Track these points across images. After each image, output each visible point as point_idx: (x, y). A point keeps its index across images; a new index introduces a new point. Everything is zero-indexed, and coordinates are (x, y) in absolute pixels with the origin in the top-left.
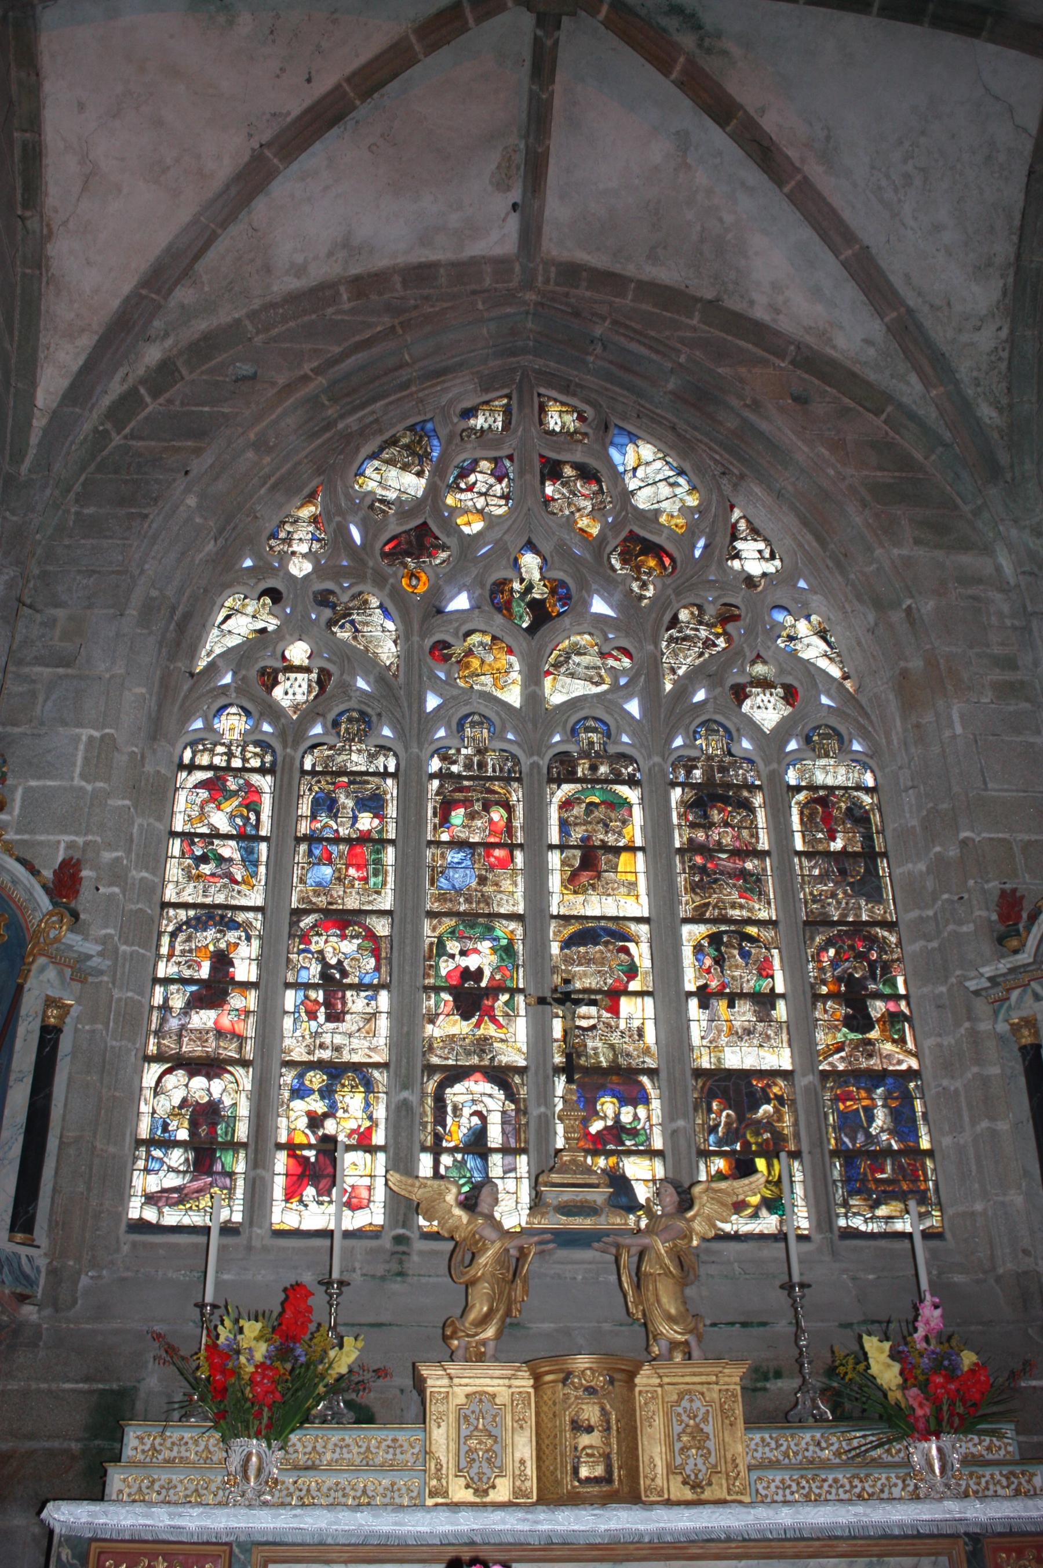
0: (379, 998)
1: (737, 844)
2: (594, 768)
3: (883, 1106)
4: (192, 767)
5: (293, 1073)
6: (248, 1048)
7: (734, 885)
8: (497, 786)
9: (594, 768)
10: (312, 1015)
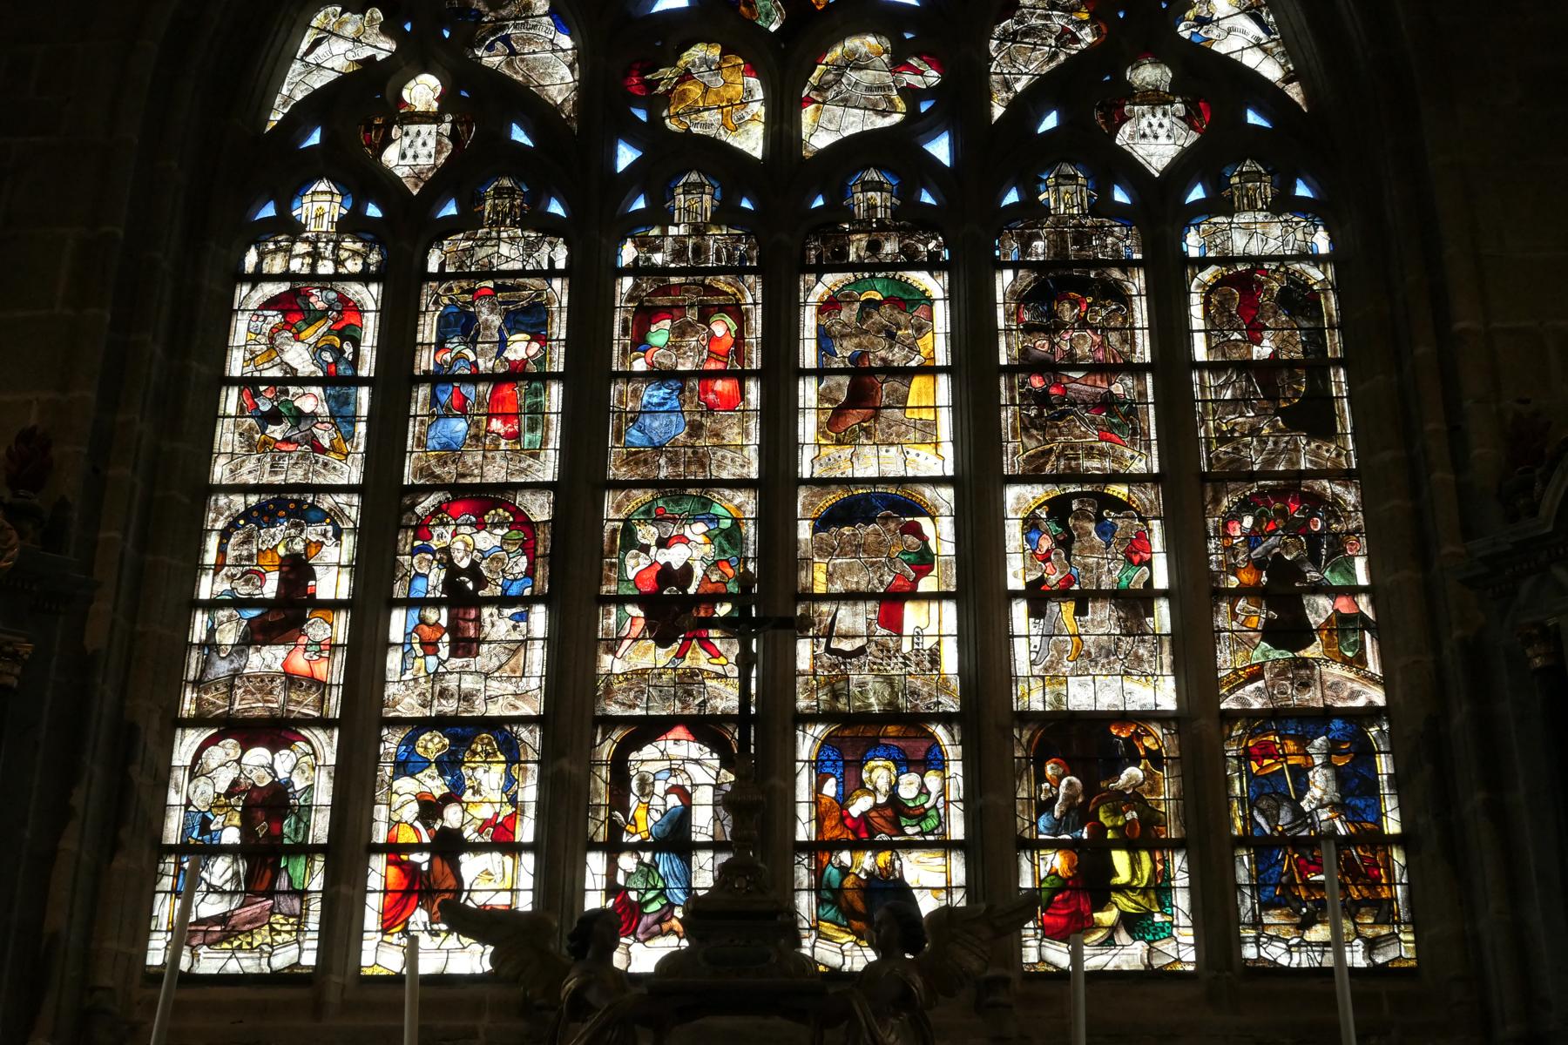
0: (532, 617)
1: (1100, 355)
2: (874, 247)
3: (1324, 766)
4: (258, 278)
5: (400, 735)
6: (333, 701)
7: (1093, 421)
8: (722, 282)
9: (874, 247)
10: (430, 647)
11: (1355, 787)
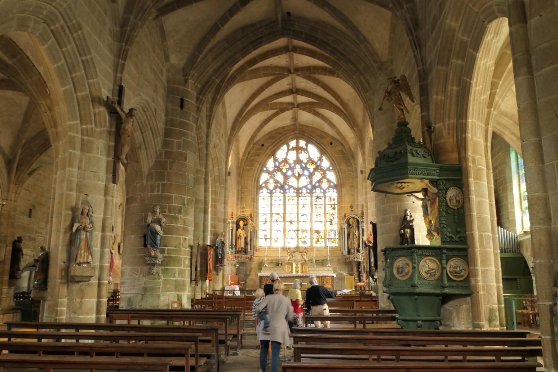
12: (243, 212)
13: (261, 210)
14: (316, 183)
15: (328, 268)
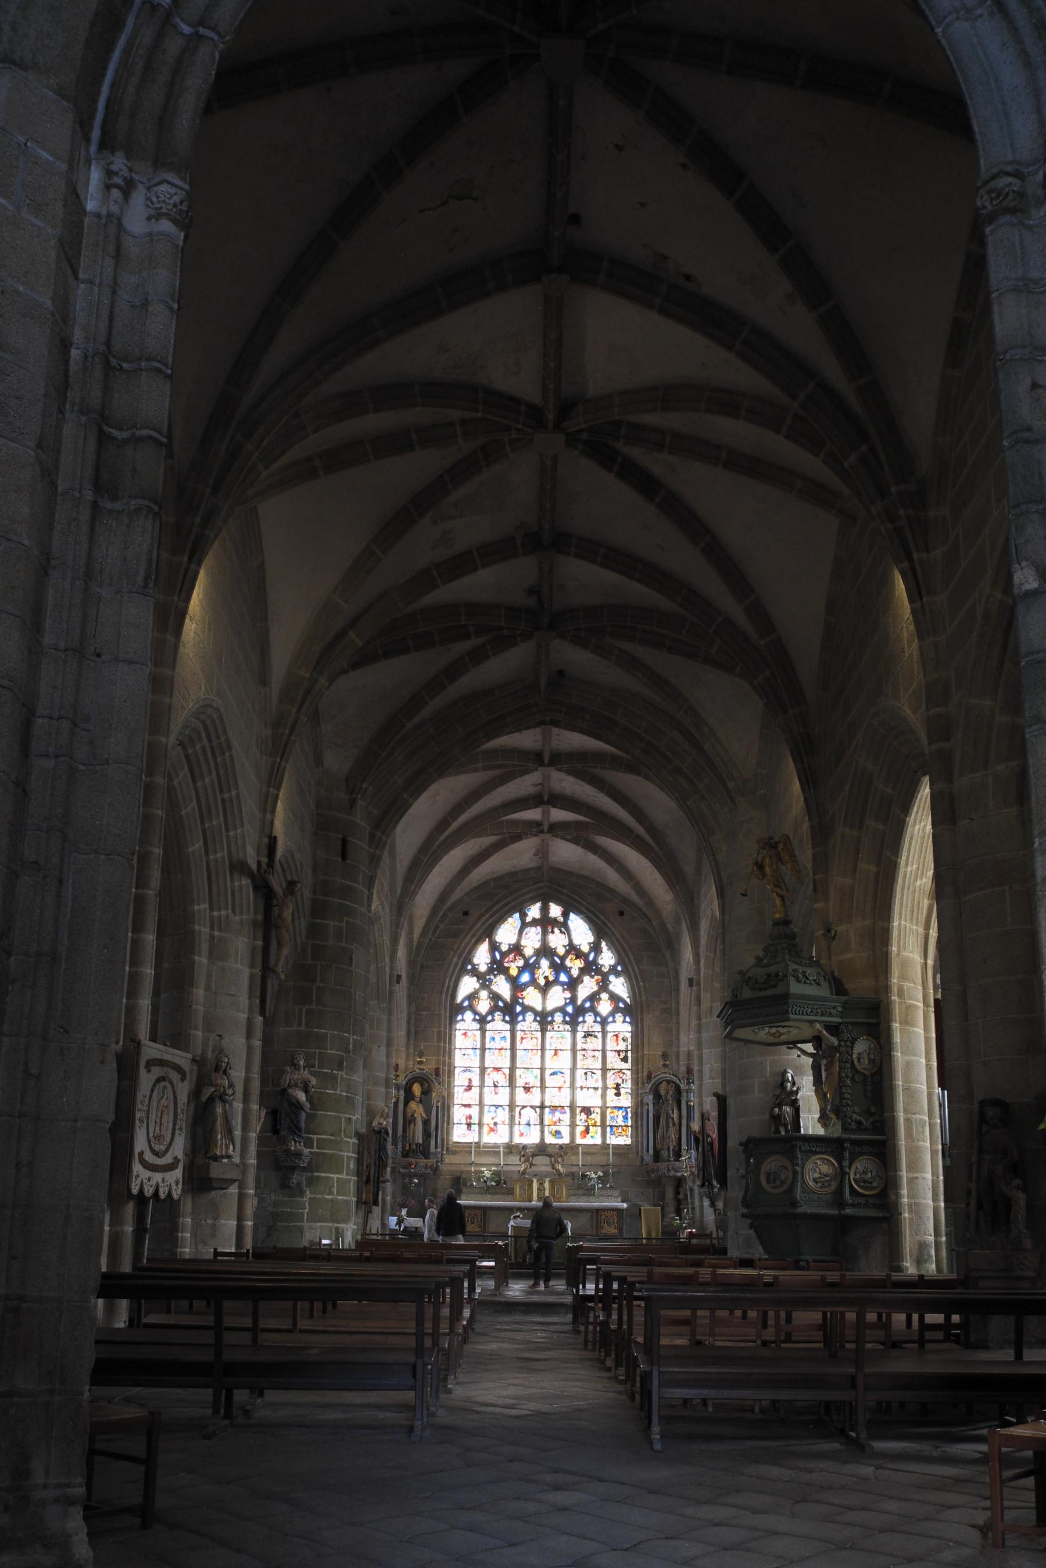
11: (625, 1118)
12: (420, 1063)
13: (459, 1060)
14: (584, 1001)
15: (611, 1192)
